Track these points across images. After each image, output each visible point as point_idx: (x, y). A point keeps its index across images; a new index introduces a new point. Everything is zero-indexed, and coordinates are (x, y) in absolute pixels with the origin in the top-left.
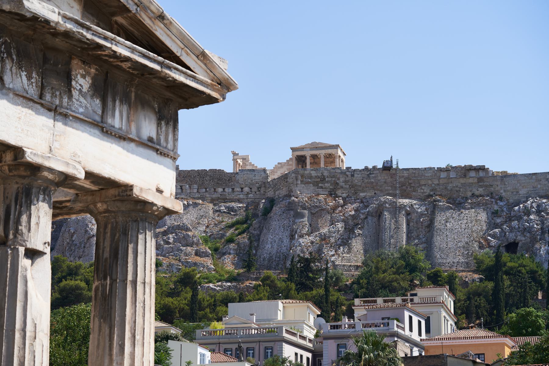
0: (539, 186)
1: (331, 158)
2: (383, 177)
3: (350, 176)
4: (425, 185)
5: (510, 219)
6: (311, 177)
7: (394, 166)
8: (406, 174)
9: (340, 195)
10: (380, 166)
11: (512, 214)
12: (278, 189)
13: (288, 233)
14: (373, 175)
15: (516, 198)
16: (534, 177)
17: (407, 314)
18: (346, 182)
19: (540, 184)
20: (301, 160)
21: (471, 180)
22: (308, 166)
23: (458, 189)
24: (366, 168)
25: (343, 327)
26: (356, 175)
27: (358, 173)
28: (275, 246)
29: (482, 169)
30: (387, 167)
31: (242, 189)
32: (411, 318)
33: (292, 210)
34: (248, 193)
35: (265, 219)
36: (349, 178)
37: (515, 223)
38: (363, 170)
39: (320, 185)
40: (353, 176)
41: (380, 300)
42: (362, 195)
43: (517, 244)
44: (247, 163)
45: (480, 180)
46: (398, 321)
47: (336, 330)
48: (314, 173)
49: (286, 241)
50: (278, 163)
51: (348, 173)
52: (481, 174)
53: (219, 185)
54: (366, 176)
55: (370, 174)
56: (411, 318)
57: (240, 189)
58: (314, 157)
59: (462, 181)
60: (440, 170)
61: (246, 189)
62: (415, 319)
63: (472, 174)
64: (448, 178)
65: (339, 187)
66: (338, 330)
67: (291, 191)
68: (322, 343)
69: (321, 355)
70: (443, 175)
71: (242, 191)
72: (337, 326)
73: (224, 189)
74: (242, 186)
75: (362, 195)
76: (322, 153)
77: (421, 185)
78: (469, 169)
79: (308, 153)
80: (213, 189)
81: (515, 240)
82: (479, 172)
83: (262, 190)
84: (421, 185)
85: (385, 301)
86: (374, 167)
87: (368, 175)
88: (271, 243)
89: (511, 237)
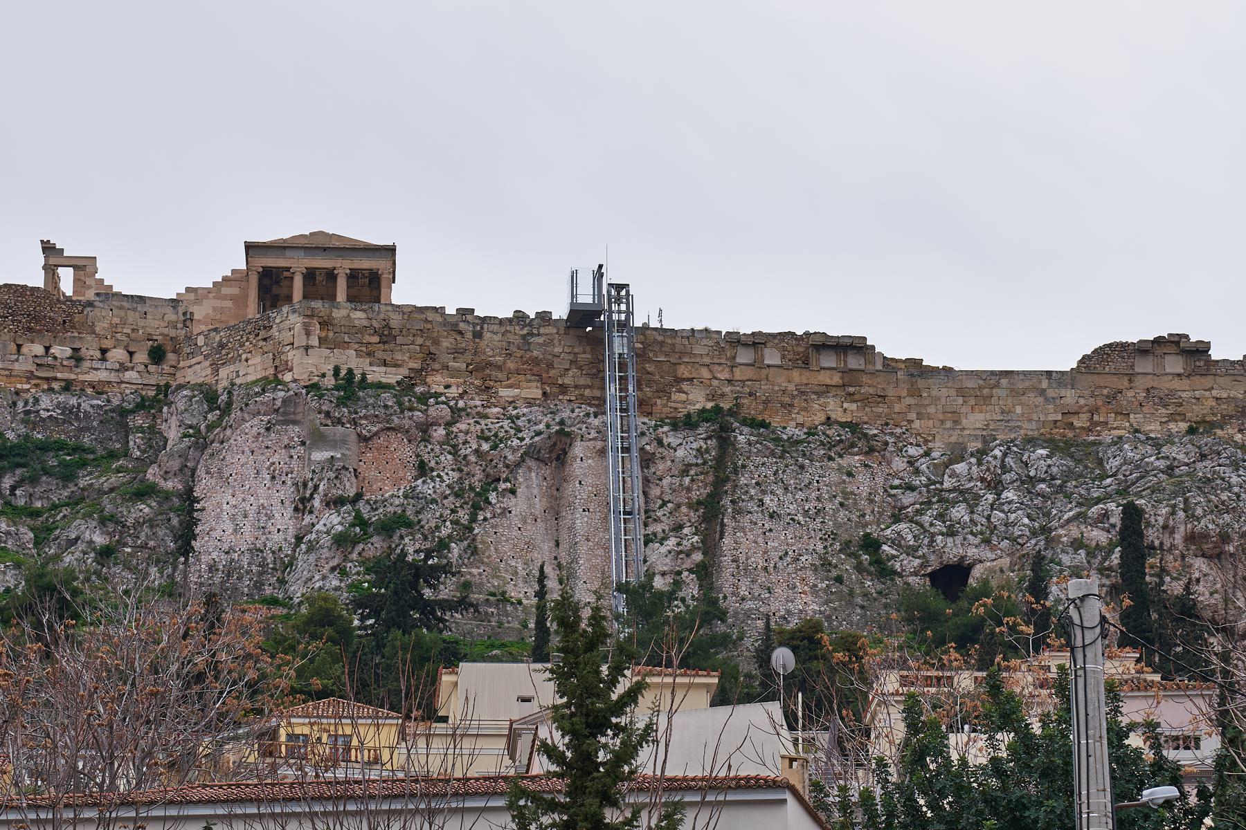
0: (1019, 410)
3: (469, 335)
4: (691, 380)
9: (441, 389)
11: (946, 485)
12: (233, 361)
13: (288, 493)
14: (540, 340)
15: (953, 439)
16: (1004, 382)
19: (1022, 404)
21: (825, 378)
22: (341, 296)
23: (787, 400)
24: (520, 317)
26: (487, 335)
27: (496, 328)
29: (857, 346)
31: (104, 351)
33: (295, 422)
34: (123, 368)
37: (959, 512)
38: (510, 320)
39: (379, 354)
40: (478, 335)
42: (506, 393)
43: (970, 568)
44: (89, 281)
50: (188, 289)
51: (462, 326)
52: (854, 362)
53: (31, 332)
54: (518, 341)
55: (532, 335)
57: (98, 354)
58: (310, 275)
61: (118, 354)
63: (829, 360)
65: (437, 366)
70: (744, 356)
71: (103, 359)
73: (47, 349)
74: (107, 344)
75: (506, 393)
76: (343, 266)
77: (679, 380)
78: (821, 344)
80: (13, 347)
81: (963, 558)
82: (846, 355)
84: (679, 380)
86: (544, 317)
87: (523, 337)
88: (233, 518)
89: (953, 550)
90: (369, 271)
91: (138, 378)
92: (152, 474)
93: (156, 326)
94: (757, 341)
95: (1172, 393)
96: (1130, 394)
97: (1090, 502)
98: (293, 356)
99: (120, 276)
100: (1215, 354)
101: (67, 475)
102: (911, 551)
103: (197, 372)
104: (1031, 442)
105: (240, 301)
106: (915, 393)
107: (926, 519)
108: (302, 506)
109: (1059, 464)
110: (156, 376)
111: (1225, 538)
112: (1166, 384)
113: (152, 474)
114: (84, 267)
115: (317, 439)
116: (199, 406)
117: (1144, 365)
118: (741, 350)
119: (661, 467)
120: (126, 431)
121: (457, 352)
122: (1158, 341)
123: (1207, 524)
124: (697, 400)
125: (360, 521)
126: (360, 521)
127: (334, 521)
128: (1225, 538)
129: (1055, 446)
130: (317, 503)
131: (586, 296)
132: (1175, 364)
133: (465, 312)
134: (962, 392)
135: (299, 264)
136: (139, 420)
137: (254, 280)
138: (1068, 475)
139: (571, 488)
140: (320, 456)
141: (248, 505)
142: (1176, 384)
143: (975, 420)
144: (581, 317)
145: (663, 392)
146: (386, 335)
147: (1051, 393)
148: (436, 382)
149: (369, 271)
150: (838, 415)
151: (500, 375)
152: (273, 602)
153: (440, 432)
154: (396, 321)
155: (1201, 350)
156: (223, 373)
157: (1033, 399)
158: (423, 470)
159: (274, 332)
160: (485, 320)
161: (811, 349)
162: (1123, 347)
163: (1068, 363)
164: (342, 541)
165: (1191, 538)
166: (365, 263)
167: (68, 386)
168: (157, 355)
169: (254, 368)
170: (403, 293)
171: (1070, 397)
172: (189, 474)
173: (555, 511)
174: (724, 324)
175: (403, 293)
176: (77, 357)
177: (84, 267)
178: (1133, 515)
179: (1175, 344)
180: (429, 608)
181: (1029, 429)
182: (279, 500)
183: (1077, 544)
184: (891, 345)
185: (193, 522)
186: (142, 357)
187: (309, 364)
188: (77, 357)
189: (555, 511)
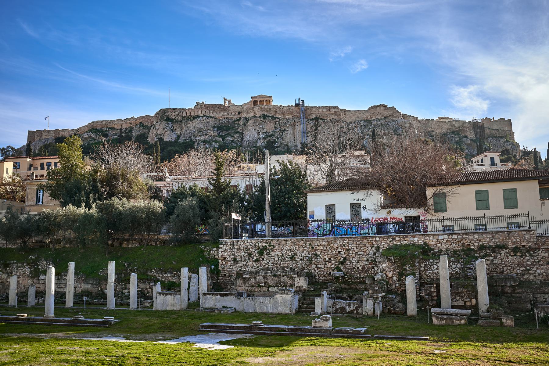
2: (296, 110)
6: (265, 108)
18: (280, 111)
20: (255, 102)
21: (332, 112)
24: (289, 106)
29: (337, 108)
42: (287, 117)
48: (266, 107)
49: (256, 135)
52: (336, 110)
58: (261, 101)
59: (328, 112)
60: (319, 107)
61: (233, 113)
63: (333, 110)
64: (322, 111)
70: (321, 110)
75: (287, 117)
76: (265, 99)
79: (259, 99)
90: (268, 100)
91: (236, 117)
92: (238, 130)
93: (239, 109)
94: (322, 107)
97: (370, 129)
98: (257, 113)
99: (234, 102)
101: (227, 131)
103: (244, 115)
104: (362, 120)
105: (251, 105)
108: (259, 133)
109: (365, 123)
110: (239, 116)
111: (389, 133)
112: (381, 111)
113: (238, 130)
114: (229, 101)
115: (260, 124)
116: (245, 120)
117: (378, 108)
119: (309, 126)
120: (235, 124)
121: (280, 111)
124: (314, 116)
125: (266, 135)
126: (266, 135)
127: (263, 135)
128: (389, 133)
129: (365, 121)
131: (297, 103)
132: (382, 108)
133: (281, 105)
134: (352, 114)
135: (259, 99)
136: (237, 122)
138: (367, 125)
139: (296, 130)
140: (261, 126)
141: (251, 134)
143: (354, 118)
144: (297, 105)
145: (309, 115)
146: (270, 109)
148: (277, 115)
149: (268, 100)
152: (255, 147)
153: (277, 123)
154: (271, 107)
155: (386, 106)
157: (362, 114)
158: (275, 127)
161: (329, 108)
164: (264, 138)
165: (384, 133)
167: (227, 118)
168: (239, 113)
169: (252, 115)
170: (273, 103)
171: (367, 114)
172: (243, 130)
173: (294, 133)
174: (318, 105)
175: (273, 103)
176: (228, 114)
177: (229, 101)
179: (383, 105)
180: (275, 147)
182: (255, 133)
183: (368, 135)
184: (342, 107)
185: (243, 137)
186: (237, 114)
187: (259, 114)
188: (228, 114)
189: (294, 133)
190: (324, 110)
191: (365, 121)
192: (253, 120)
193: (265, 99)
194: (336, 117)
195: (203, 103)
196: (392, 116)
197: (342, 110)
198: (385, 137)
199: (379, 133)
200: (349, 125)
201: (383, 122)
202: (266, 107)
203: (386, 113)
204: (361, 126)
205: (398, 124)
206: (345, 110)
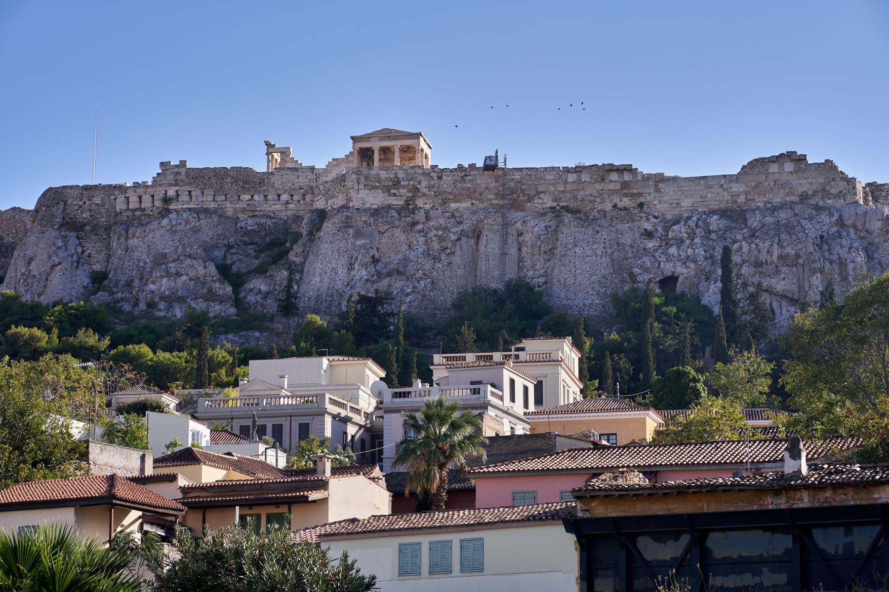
0: (709, 195)
1: (409, 151)
2: (484, 180)
3: (435, 178)
4: (545, 192)
5: (666, 242)
7: (501, 165)
8: (517, 177)
9: (422, 206)
10: (480, 164)
11: (670, 236)
12: (332, 197)
13: (344, 261)
14: (470, 178)
15: (677, 212)
16: (702, 182)
17: (507, 375)
19: (711, 193)
20: (365, 155)
21: (611, 186)
22: (376, 163)
23: (592, 199)
24: (460, 167)
25: (413, 394)
26: (444, 178)
27: (449, 173)
28: (326, 280)
30: (490, 166)
31: (279, 196)
32: (512, 382)
33: (351, 227)
34: (287, 203)
35: (312, 241)
36: (435, 181)
37: (673, 250)
38: (456, 169)
39: (392, 191)
40: (440, 178)
41: (470, 357)
43: (677, 278)
44: (287, 159)
45: (625, 185)
46: (493, 385)
47: (402, 400)
48: (383, 174)
49: (342, 273)
50: (333, 159)
51: (432, 174)
52: (627, 177)
53: (245, 190)
54: (459, 179)
55: (466, 175)
56: (512, 382)
57: (276, 197)
58: (385, 151)
59: (599, 187)
60: (567, 170)
61: (285, 197)
62: (519, 383)
63: (614, 176)
64: (579, 182)
65: (420, 194)
66: (406, 399)
67: (349, 200)
68: (382, 417)
69: (381, 437)
70: (571, 178)
71: (279, 200)
72: (404, 393)
73: (252, 196)
74: (280, 192)
75: (453, 206)
77: (539, 193)
78: (611, 169)
79: (376, 145)
80: (236, 197)
81: (673, 273)
82: (623, 174)
83: (308, 198)
84: (539, 193)
85: (478, 358)
86: (472, 166)
87: (462, 177)
88: (320, 275)
89: (668, 268)
93: (303, 180)
94: (579, 170)
95: (787, 182)
96: (766, 184)
98: (353, 194)
100: (810, 161)
102: (647, 270)
103: (320, 204)
104: (713, 212)
106: (657, 190)
107: (657, 254)
108: (351, 267)
109: (723, 223)
111: (798, 256)
112: (785, 178)
117: (774, 168)
118: (570, 175)
122: (782, 155)
123: (790, 250)
130: (356, 266)
132: (789, 167)
137: (356, 154)
138: (728, 229)
140: (359, 243)
142: (790, 177)
143: (686, 203)
145: (530, 199)
147: (725, 186)
148: (420, 202)
150: (621, 204)
151: (451, 197)
155: (803, 158)
156: (330, 202)
159: (346, 183)
160: (443, 170)
162: (763, 159)
163: (735, 170)
165: (781, 257)
166: (407, 142)
169: (339, 201)
171: (735, 188)
178: (727, 252)
179: (791, 156)
181: (714, 206)
184: (646, 168)
190: (585, 177)
191: (724, 213)
192: (338, 219)
193: (397, 144)
194: (626, 202)
195: (183, 163)
196: (824, 191)
197: (647, 178)
198: (784, 269)
199: (763, 257)
200: (667, 229)
201: (783, 215)
202: (383, 174)
203: (805, 184)
204: (710, 232)
205: (841, 222)
206: (660, 179)
